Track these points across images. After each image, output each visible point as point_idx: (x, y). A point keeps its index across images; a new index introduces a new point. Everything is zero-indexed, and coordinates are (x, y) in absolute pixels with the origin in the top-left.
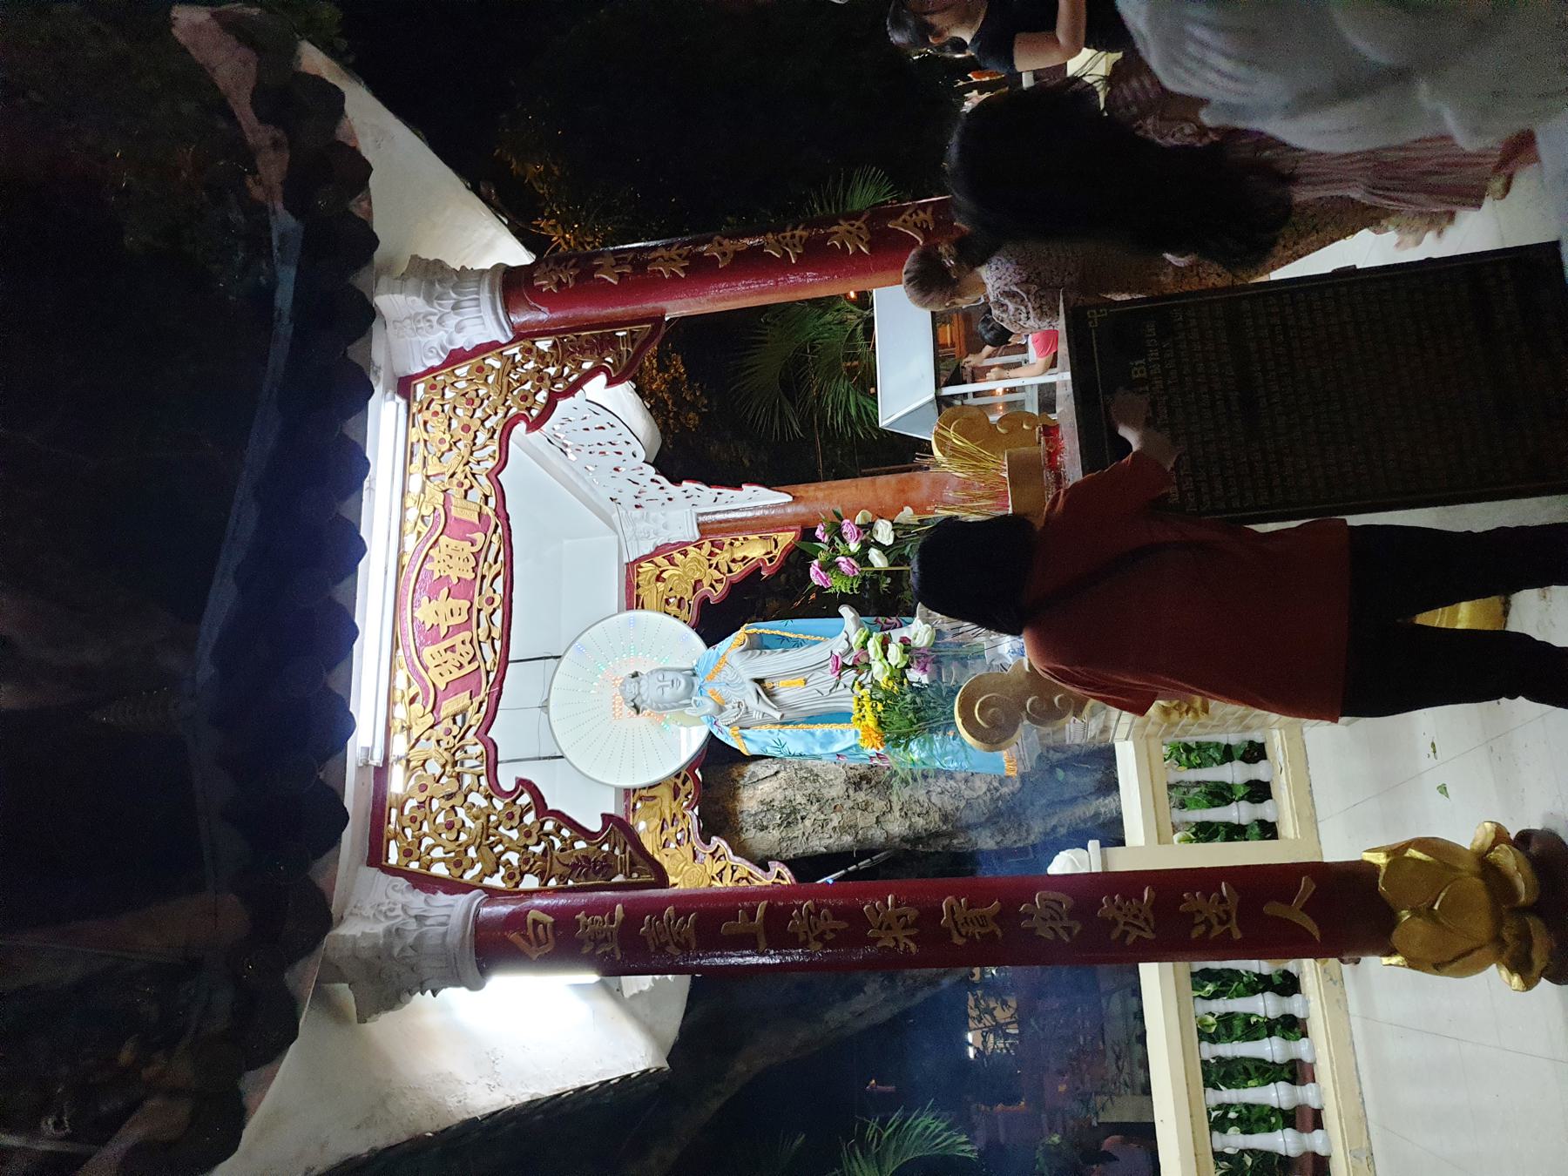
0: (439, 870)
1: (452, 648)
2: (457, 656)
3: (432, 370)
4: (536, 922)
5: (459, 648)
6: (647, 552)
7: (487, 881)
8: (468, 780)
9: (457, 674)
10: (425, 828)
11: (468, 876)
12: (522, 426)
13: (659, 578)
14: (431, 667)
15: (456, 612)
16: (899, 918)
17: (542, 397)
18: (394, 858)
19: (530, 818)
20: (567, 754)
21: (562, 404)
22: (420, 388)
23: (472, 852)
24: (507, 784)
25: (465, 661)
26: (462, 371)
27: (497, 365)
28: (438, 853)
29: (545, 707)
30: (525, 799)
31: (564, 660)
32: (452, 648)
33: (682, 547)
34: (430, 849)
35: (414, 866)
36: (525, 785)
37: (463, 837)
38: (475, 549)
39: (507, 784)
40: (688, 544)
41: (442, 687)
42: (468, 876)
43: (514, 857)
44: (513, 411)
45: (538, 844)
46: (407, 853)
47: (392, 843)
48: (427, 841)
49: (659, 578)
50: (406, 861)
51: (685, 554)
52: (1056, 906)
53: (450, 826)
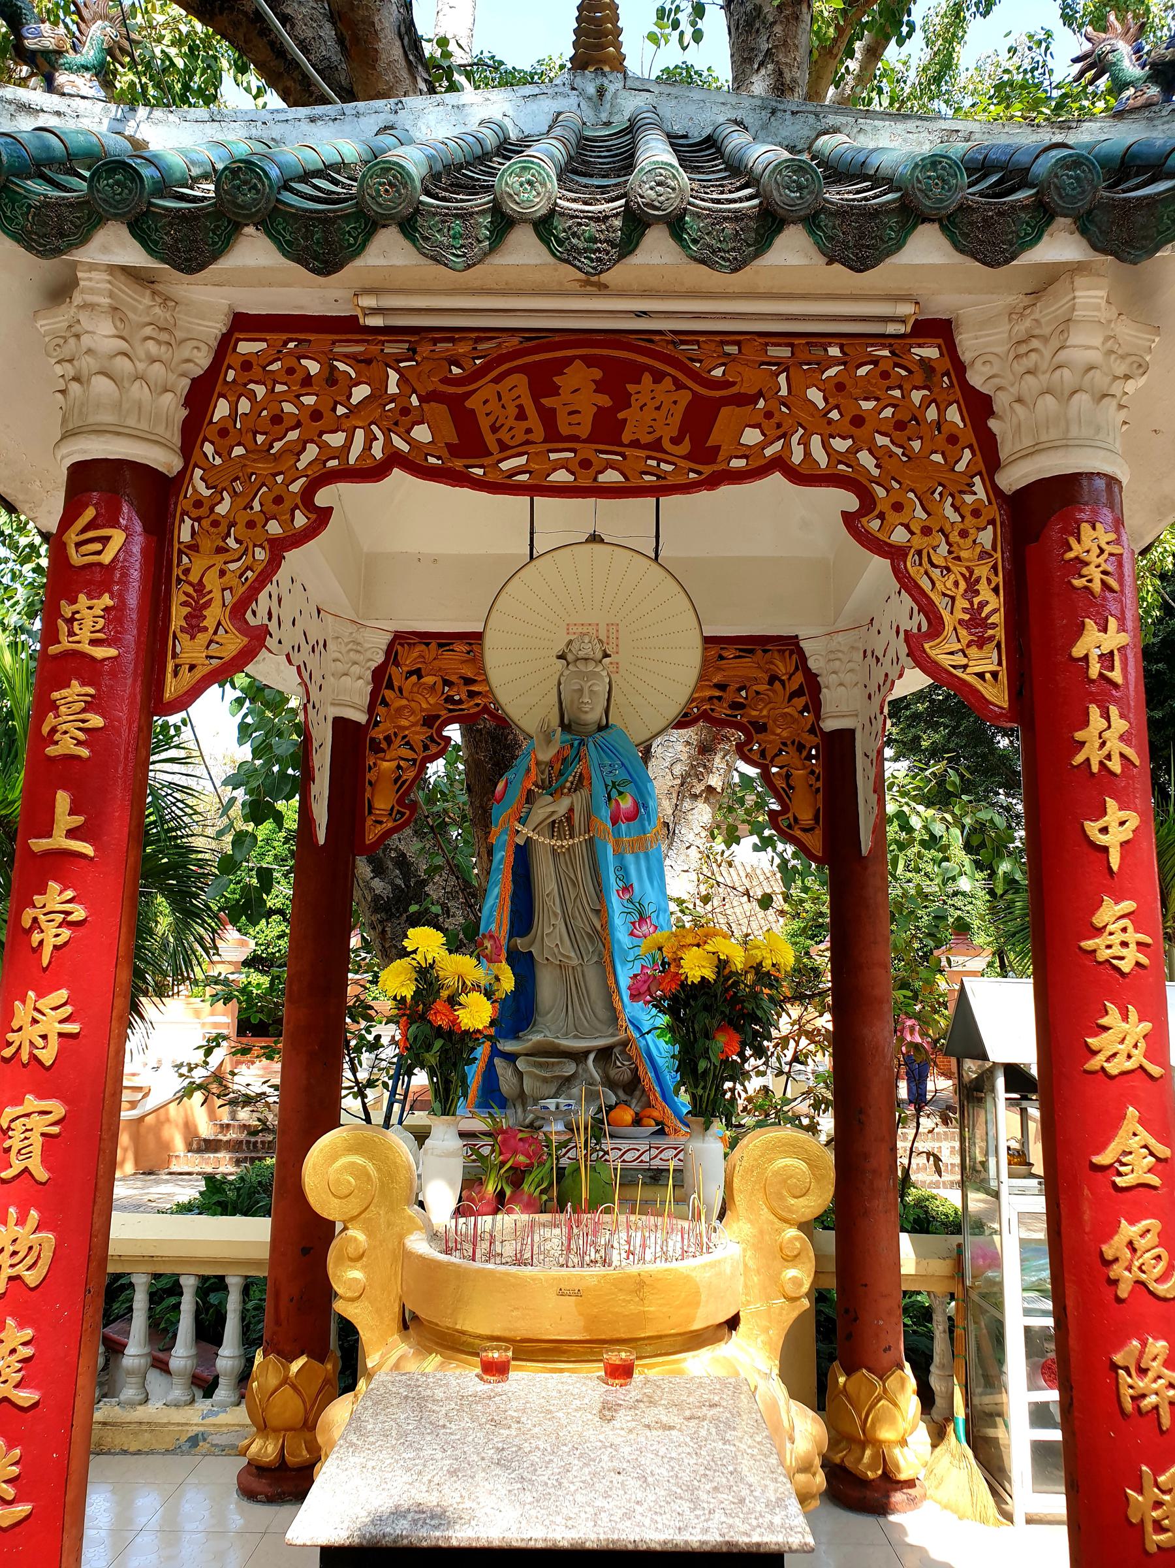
0: (222, 409)
1: (521, 416)
2: (511, 422)
3: (959, 368)
4: (105, 540)
5: (525, 425)
6: (812, 664)
7: (198, 472)
8: (336, 440)
9: (484, 424)
10: (279, 388)
11: (208, 448)
12: (851, 502)
13: (773, 679)
14: (498, 387)
15: (575, 419)
16: (44, 1037)
17: (899, 536)
18: (244, 348)
19: (274, 528)
20: (534, 563)
21: (880, 565)
22: (931, 353)
23: (238, 451)
24: (322, 498)
25: (503, 435)
26: (953, 415)
27: (961, 467)
28: (244, 406)
29: (595, 538)
30: (300, 520)
31: (654, 565)
32: (521, 416)
33: (815, 706)
34: (252, 396)
35: (231, 375)
36: (323, 516)
37: (260, 439)
38: (666, 444)
39: (322, 498)
40: (818, 717)
41: (469, 404)
42: (208, 448)
43: (222, 509)
44: (881, 492)
45: (237, 541)
46: (246, 365)
47: (264, 345)
48: (260, 391)
49: (773, 679)
50: (238, 365)
51: (806, 708)
52: (29, 1261)
53: (277, 419)
